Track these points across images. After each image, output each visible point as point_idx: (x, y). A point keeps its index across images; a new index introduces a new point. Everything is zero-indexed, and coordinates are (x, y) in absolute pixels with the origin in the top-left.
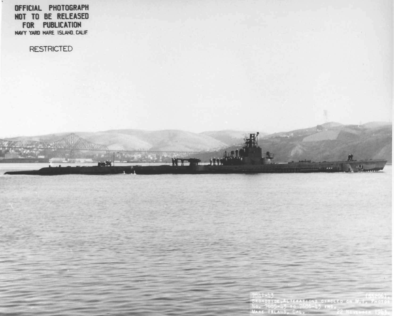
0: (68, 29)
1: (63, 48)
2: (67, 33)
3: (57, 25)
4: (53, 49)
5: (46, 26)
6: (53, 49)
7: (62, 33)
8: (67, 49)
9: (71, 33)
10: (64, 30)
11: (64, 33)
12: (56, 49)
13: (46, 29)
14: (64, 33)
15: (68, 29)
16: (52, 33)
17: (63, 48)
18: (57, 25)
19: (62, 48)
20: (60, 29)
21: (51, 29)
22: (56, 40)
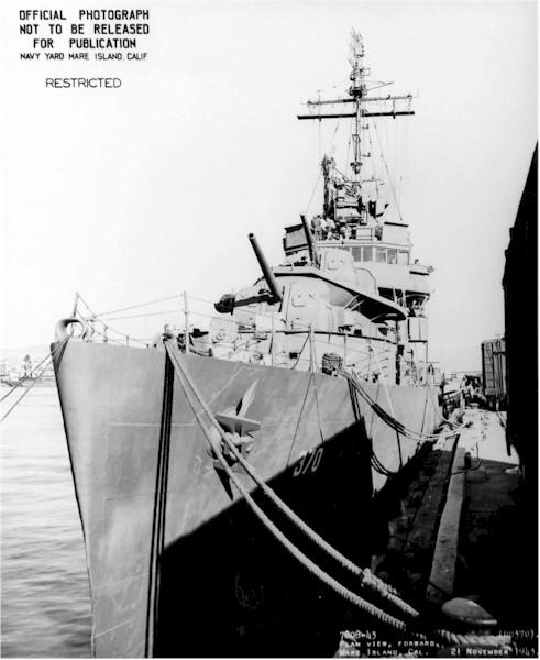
0: (114, 51)
1: (106, 82)
2: (110, 57)
3: (94, 44)
4: (87, 83)
5: (74, 45)
6: (87, 83)
7: (102, 58)
8: (111, 83)
9: (118, 56)
10: (107, 51)
11: (106, 57)
12: (93, 83)
13: (75, 50)
14: (106, 57)
15: (114, 51)
16: (85, 56)
17: (106, 82)
18: (94, 44)
19: (103, 81)
20: (99, 50)
21: (83, 50)
22: (91, 67)
